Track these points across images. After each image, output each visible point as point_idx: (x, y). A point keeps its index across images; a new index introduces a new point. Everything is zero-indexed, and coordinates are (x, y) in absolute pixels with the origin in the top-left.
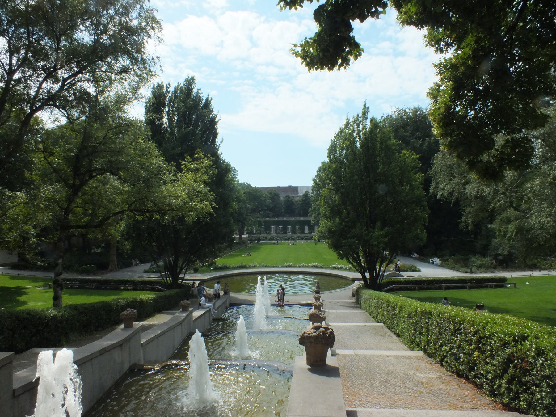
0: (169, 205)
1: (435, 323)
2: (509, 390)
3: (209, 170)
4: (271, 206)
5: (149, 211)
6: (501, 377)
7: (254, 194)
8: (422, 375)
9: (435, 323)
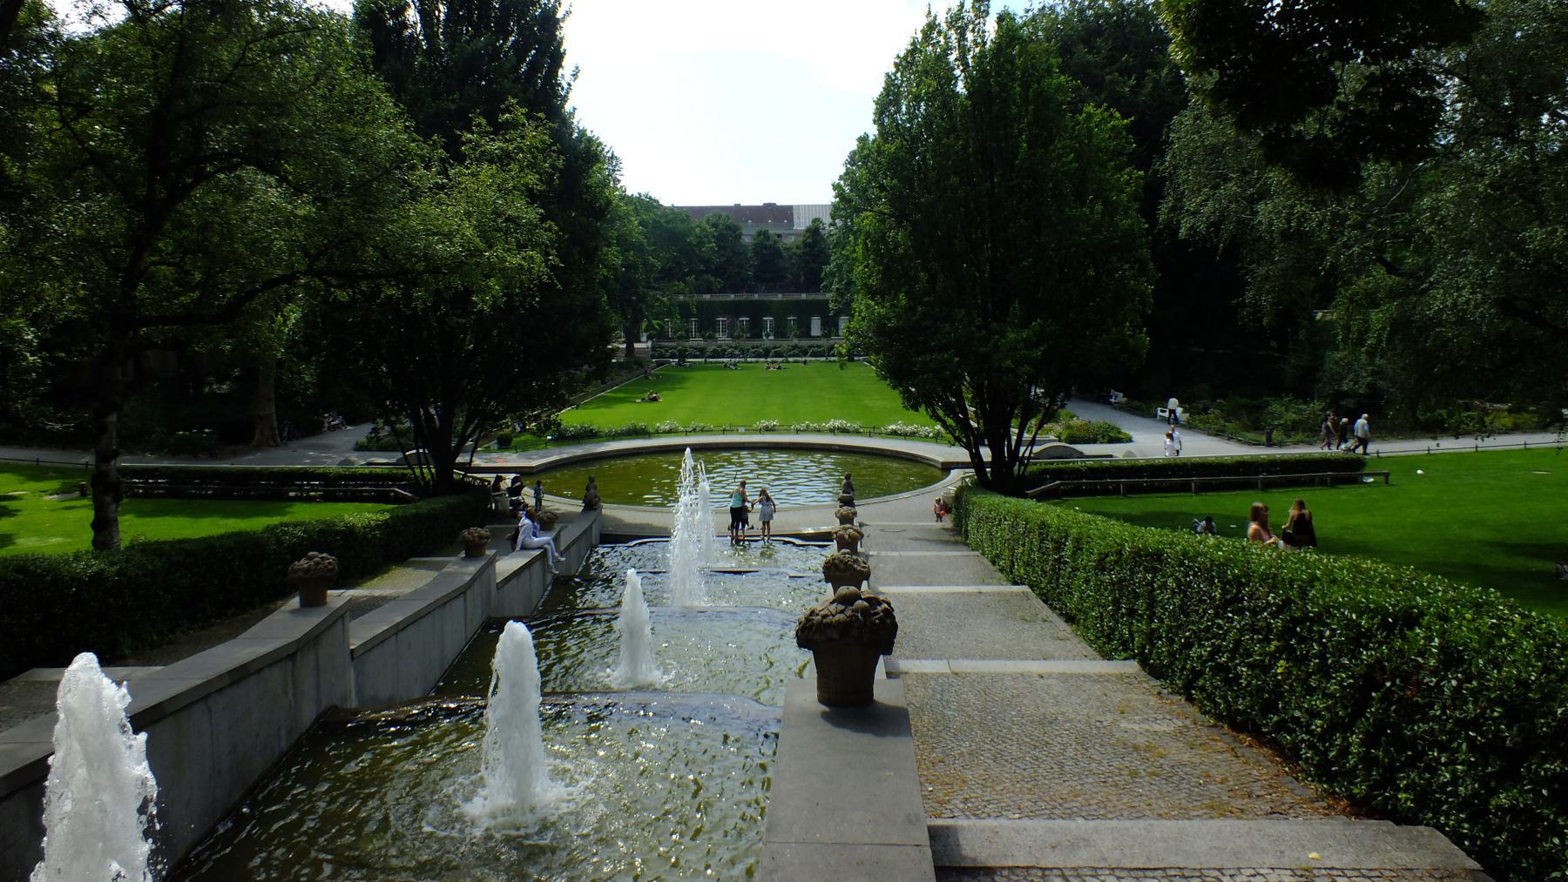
0: (427, 258)
1: (1171, 583)
2: (1368, 761)
3: (540, 157)
4: (716, 260)
5: (367, 276)
6: (1347, 728)
8: (1136, 727)
9: (1171, 583)
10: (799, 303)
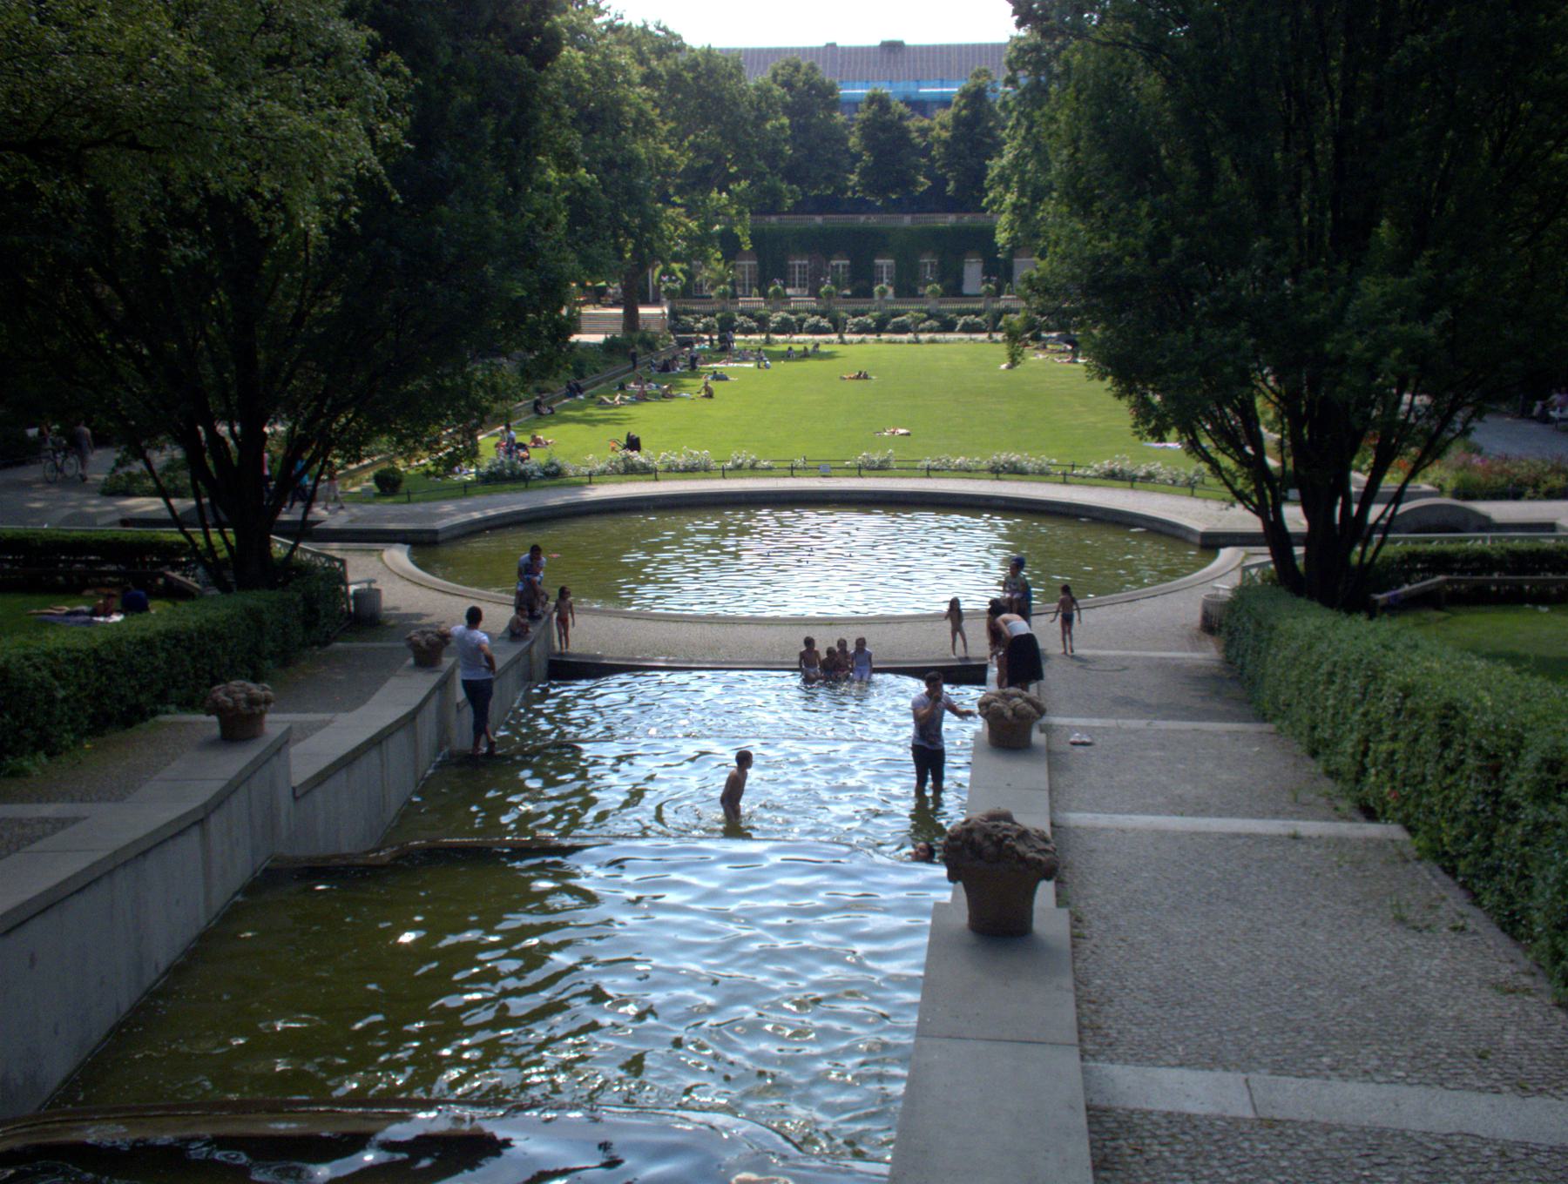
7: (701, 86)
10: (939, 234)
